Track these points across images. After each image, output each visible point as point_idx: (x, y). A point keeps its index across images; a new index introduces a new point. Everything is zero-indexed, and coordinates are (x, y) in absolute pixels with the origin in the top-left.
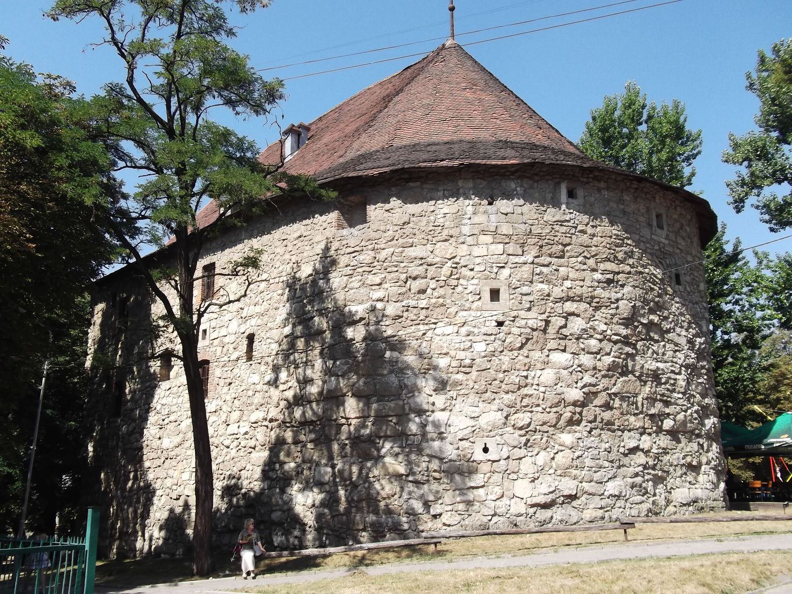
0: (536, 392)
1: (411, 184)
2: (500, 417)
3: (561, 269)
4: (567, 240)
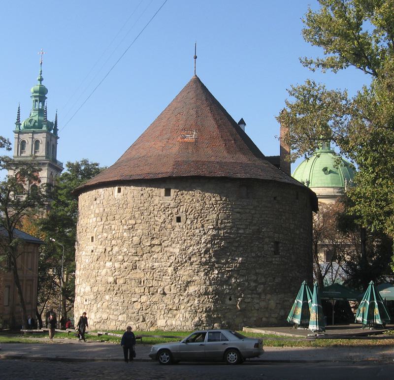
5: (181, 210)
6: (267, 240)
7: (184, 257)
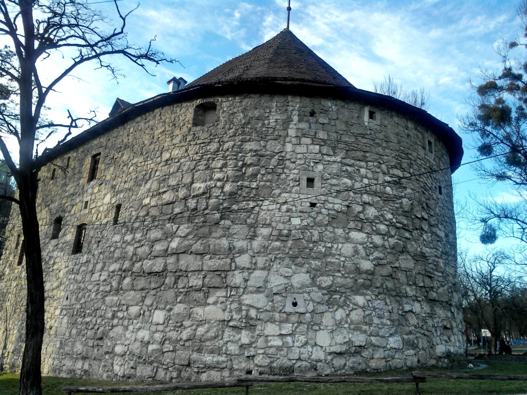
0: (337, 261)
1: (252, 95)
2: (308, 278)
3: (361, 170)
4: (368, 149)
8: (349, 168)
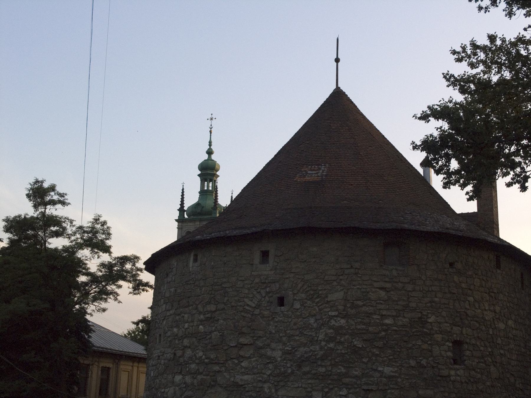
5: (286, 286)
6: (439, 337)
7: (288, 365)
8: (177, 317)
